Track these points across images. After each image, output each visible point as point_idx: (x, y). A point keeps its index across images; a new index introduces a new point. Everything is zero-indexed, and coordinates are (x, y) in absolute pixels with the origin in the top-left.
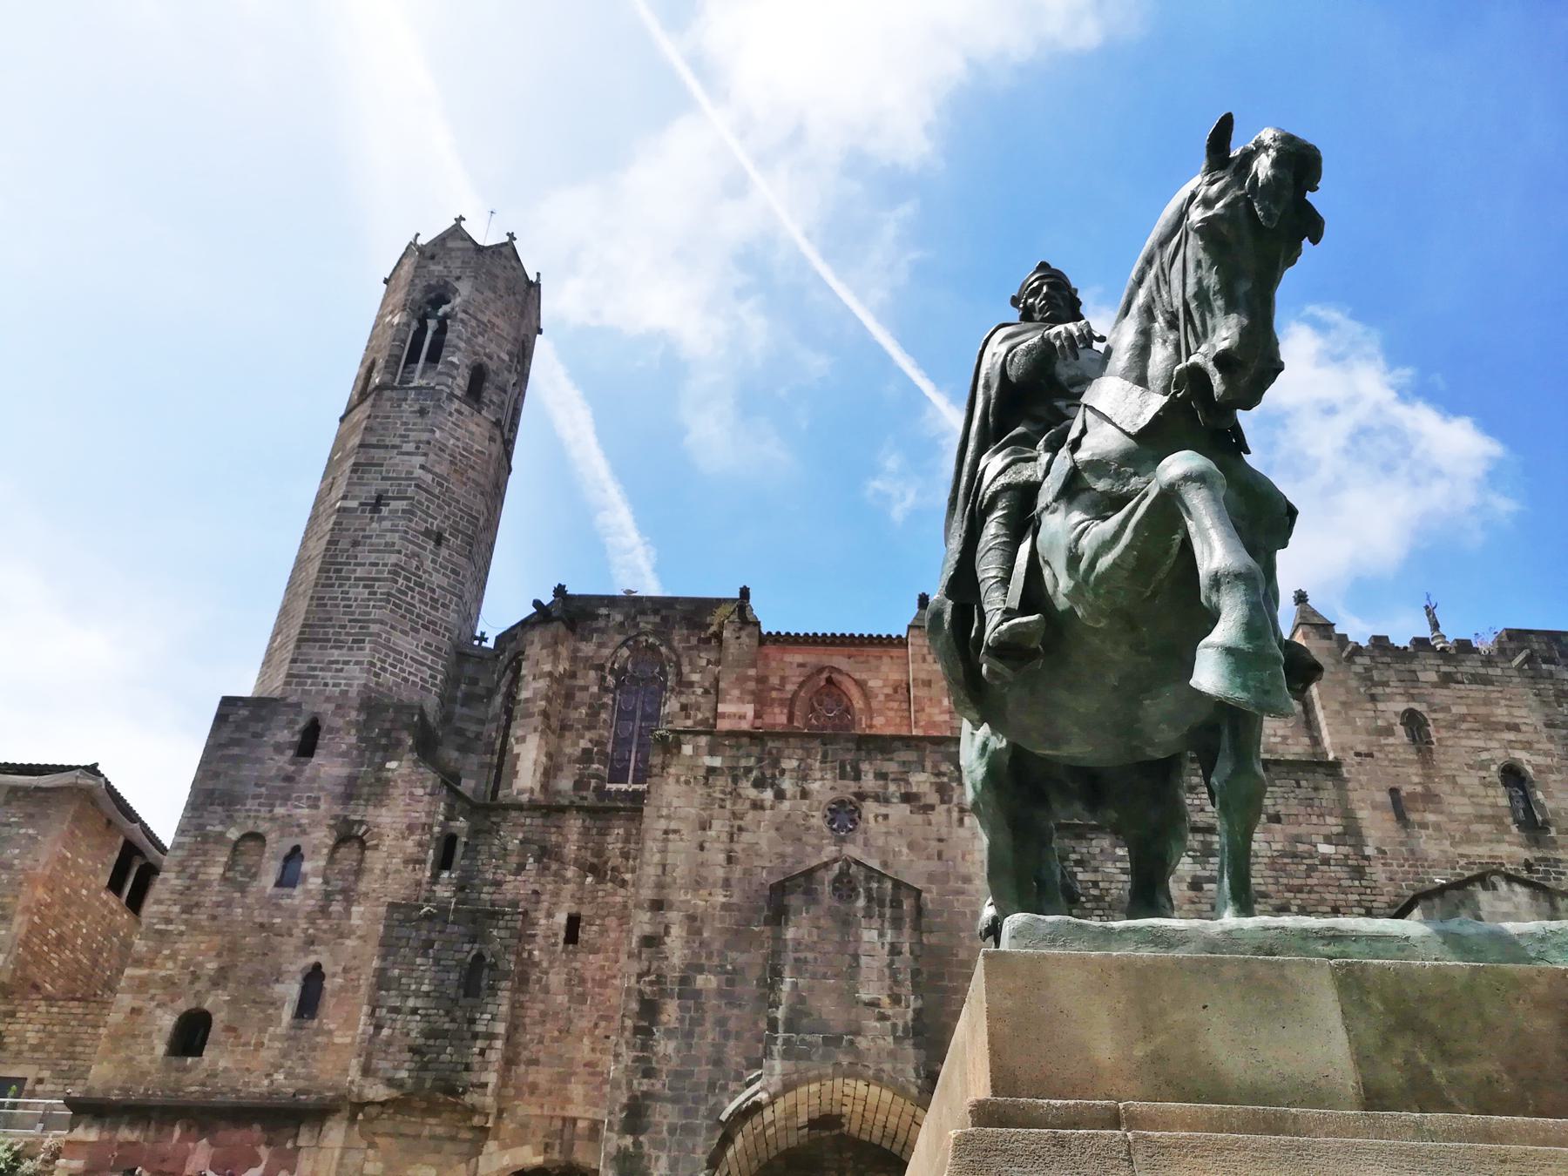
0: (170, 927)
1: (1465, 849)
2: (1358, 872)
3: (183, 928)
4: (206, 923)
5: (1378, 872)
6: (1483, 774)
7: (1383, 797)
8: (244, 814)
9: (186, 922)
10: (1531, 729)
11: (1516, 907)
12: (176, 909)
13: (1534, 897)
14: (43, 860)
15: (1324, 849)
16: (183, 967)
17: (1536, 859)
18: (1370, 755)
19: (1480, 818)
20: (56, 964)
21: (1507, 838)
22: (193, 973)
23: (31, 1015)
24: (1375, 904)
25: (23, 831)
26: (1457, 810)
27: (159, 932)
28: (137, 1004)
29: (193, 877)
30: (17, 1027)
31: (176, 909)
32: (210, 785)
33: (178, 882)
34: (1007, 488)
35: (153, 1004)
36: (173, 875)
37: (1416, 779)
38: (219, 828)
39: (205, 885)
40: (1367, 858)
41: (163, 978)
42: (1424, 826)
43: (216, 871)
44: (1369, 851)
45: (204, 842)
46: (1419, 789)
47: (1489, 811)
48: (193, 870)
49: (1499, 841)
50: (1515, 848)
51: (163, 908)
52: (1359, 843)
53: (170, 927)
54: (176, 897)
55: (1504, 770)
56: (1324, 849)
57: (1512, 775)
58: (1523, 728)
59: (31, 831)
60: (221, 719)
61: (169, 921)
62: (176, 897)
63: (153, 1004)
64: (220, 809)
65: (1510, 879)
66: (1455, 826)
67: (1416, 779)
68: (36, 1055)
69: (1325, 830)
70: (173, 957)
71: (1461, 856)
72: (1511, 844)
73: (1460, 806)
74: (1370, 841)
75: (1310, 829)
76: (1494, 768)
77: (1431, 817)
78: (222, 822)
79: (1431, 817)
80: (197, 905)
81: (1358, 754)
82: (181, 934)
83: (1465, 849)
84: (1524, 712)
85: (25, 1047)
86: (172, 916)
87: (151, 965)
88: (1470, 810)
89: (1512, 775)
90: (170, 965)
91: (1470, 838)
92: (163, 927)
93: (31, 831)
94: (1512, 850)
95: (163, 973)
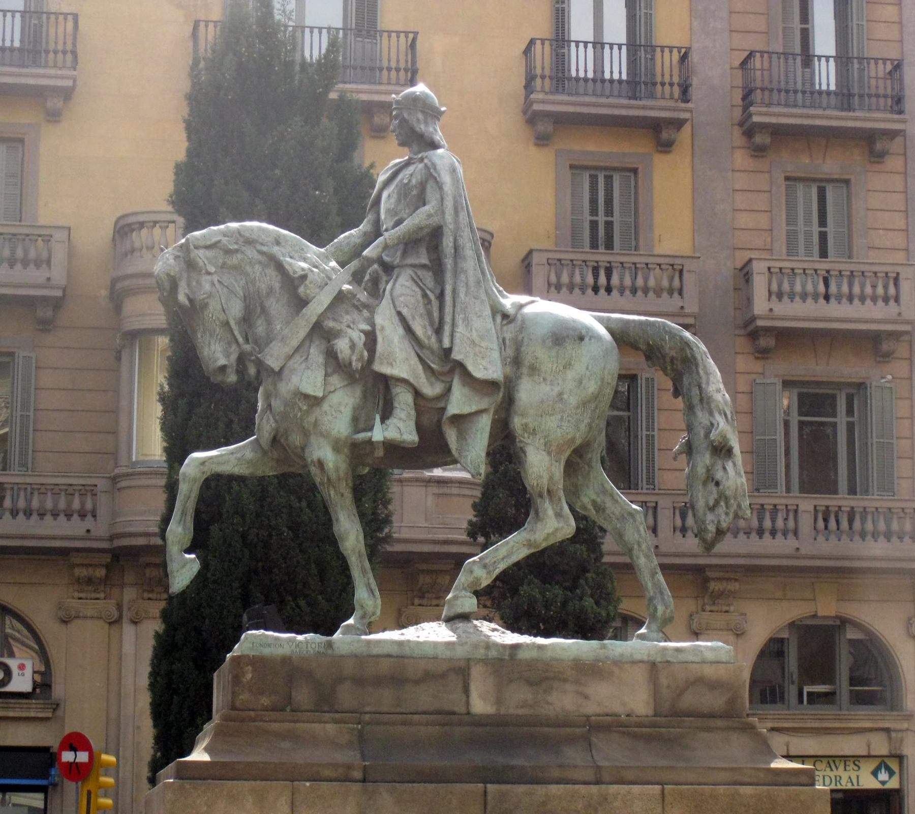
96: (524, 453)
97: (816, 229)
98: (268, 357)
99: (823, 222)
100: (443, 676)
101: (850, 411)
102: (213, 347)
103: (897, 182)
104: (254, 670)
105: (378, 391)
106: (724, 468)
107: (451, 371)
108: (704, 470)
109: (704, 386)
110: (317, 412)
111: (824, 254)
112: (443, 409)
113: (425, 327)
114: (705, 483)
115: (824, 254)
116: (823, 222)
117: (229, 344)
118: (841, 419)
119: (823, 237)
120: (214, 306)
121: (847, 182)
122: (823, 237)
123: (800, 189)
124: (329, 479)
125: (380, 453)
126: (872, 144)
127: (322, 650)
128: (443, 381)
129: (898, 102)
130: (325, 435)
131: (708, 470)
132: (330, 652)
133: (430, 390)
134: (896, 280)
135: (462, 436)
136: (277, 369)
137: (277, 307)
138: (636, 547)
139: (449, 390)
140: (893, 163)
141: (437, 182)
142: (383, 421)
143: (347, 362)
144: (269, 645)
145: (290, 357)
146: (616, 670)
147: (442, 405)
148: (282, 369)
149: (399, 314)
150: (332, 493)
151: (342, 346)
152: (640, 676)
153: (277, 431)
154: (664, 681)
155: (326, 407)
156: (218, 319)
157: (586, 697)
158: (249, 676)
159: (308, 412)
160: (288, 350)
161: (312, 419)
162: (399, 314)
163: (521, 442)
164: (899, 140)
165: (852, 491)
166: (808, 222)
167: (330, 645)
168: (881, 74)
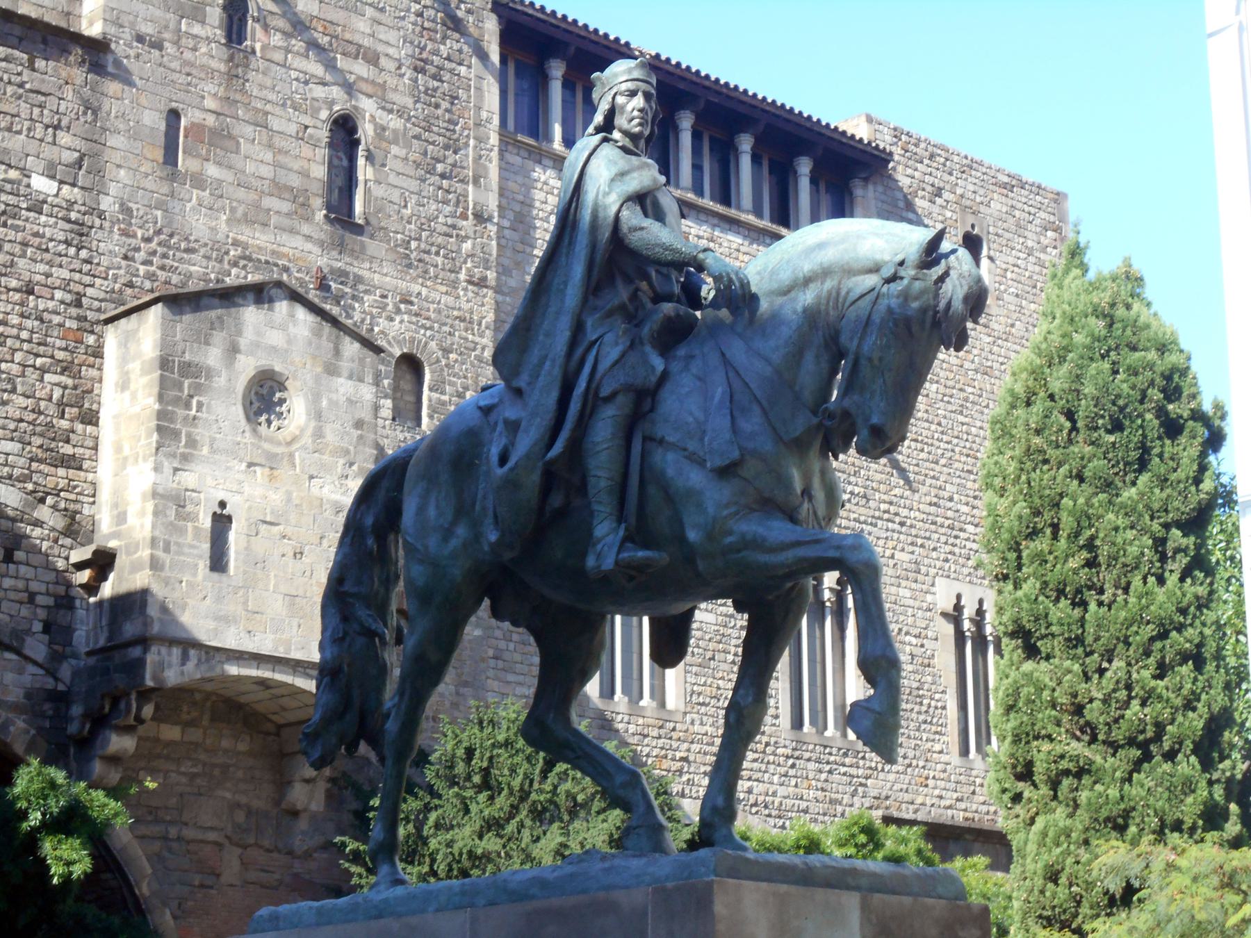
1: (246, 234)
2: (81, 232)
5: (109, 244)
6: (307, 120)
7: (154, 120)
10: (391, 66)
11: (289, 342)
13: (317, 333)
15: (41, 184)
17: (332, 271)
18: (158, 45)
19: (279, 189)
21: (306, 229)
24: (90, 291)
26: (250, 167)
34: (627, 388)
37: (210, 103)
40: (101, 215)
42: (199, 181)
44: (106, 203)
46: (211, 120)
47: (295, 181)
49: (292, 231)
50: (309, 246)
52: (95, 189)
55: (335, 122)
56: (41, 184)
57: (344, 130)
58: (383, 61)
65: (296, 297)
66: (241, 193)
67: (210, 103)
69: (49, 152)
71: (236, 243)
72: (308, 238)
73: (256, 160)
74: (113, 188)
75: (33, 147)
76: (324, 114)
77: (212, 171)
79: (212, 171)
81: (140, 39)
83: (246, 234)
84: (392, 36)
88: (266, 171)
89: (344, 130)
91: (256, 217)
94: (303, 249)
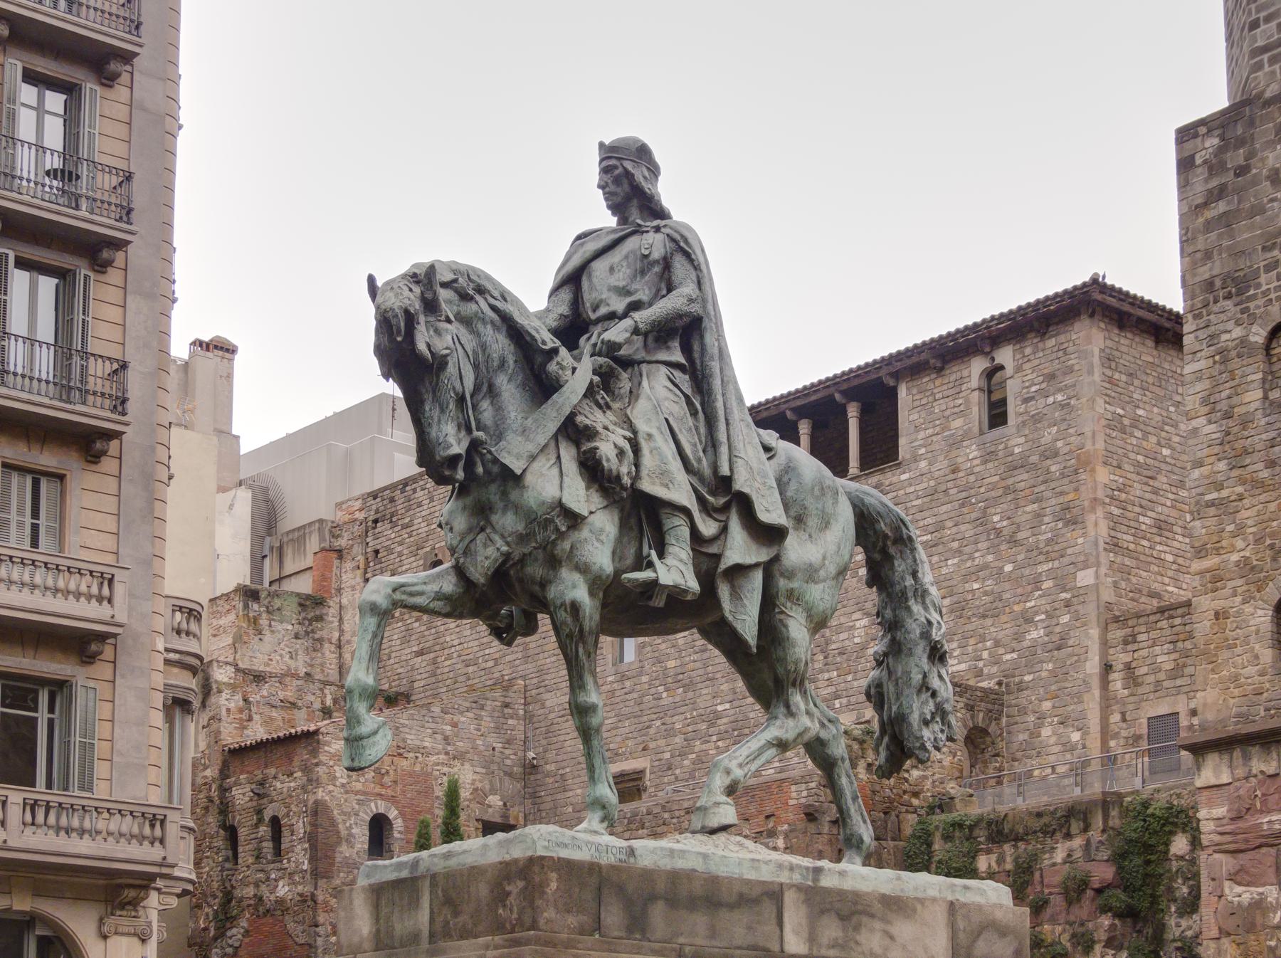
0: (1225, 493)
3: (1240, 489)
4: (1265, 474)
8: (1260, 302)
9: (1242, 481)
12: (1222, 466)
14: (1087, 430)
16: (1257, 541)
20: (1170, 558)
22: (1272, 547)
23: (1153, 634)
25: (1051, 400)
27: (1212, 504)
28: (1219, 604)
29: (1228, 415)
30: (1144, 653)
31: (1222, 466)
32: (1204, 272)
33: (1213, 427)
35: (1239, 599)
36: (1203, 420)
38: (1238, 332)
39: (1245, 423)
41: (1237, 564)
43: (1254, 396)
45: (1224, 361)
48: (1223, 406)
51: (1205, 470)
53: (1225, 493)
54: (1216, 449)
59: (1059, 397)
60: (1185, 165)
61: (1219, 487)
62: (1216, 449)
63: (1239, 599)
64: (1228, 304)
68: (1179, 682)
70: (1240, 531)
78: (1238, 323)
80: (1246, 452)
82: (1241, 498)
85: (1162, 676)
86: (1220, 477)
87: (1218, 552)
90: (1240, 544)
92: (1215, 495)
93: (1059, 397)
95: (1235, 557)
96: (786, 626)
97: (28, 520)
98: (504, 454)
99: (35, 513)
100: (756, 901)
101: (51, 710)
102: (443, 427)
103: (111, 485)
104: (559, 879)
105: (644, 516)
106: (940, 677)
107: (725, 508)
108: (920, 676)
109: (920, 575)
110: (575, 536)
111: (35, 543)
112: (717, 557)
113: (695, 445)
114: (919, 692)
115: (35, 543)
116: (35, 513)
117: (459, 427)
118: (43, 716)
119: (35, 528)
120: (451, 369)
121: (61, 477)
122: (35, 528)
123: (15, 478)
124: (581, 630)
125: (659, 602)
126: (89, 443)
127: (623, 857)
128: (716, 520)
129: (120, 403)
130: (583, 569)
131: (925, 676)
132: (632, 860)
133: (708, 528)
134: (111, 581)
135: (736, 595)
136: (518, 472)
137: (510, 390)
138: (840, 763)
139: (724, 530)
140: (108, 464)
141: (697, 268)
142: (661, 555)
143: (615, 472)
144: (566, 846)
145: (533, 458)
146: (919, 907)
147: (713, 549)
148: (524, 471)
149: (667, 420)
150: (581, 650)
151: (606, 449)
152: (939, 916)
153: (507, 556)
154: (961, 924)
155: (585, 533)
156: (454, 388)
157: (892, 938)
158: (554, 885)
159: (561, 535)
160: (531, 448)
161: (566, 545)
162: (667, 420)
163: (782, 612)
164: (114, 444)
165: (49, 785)
166: (21, 512)
167: (631, 852)
168: (99, 374)
